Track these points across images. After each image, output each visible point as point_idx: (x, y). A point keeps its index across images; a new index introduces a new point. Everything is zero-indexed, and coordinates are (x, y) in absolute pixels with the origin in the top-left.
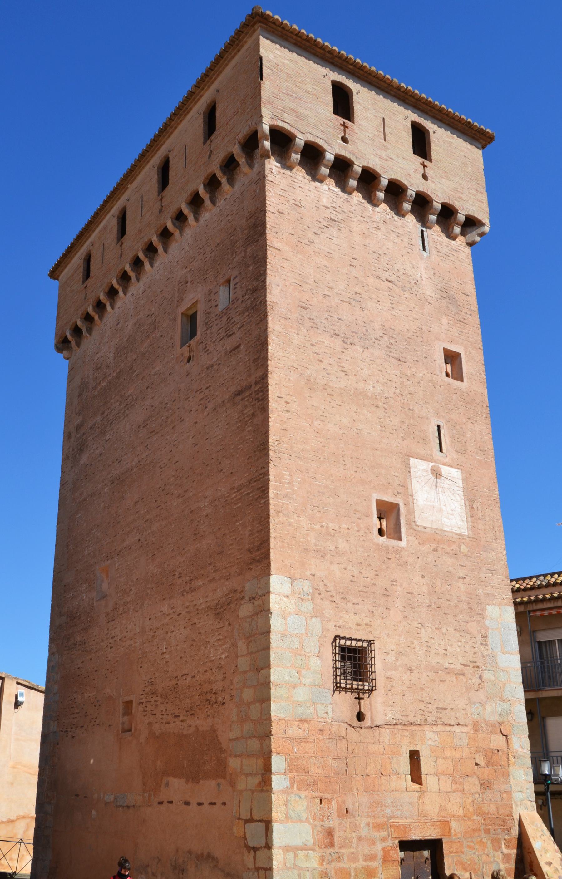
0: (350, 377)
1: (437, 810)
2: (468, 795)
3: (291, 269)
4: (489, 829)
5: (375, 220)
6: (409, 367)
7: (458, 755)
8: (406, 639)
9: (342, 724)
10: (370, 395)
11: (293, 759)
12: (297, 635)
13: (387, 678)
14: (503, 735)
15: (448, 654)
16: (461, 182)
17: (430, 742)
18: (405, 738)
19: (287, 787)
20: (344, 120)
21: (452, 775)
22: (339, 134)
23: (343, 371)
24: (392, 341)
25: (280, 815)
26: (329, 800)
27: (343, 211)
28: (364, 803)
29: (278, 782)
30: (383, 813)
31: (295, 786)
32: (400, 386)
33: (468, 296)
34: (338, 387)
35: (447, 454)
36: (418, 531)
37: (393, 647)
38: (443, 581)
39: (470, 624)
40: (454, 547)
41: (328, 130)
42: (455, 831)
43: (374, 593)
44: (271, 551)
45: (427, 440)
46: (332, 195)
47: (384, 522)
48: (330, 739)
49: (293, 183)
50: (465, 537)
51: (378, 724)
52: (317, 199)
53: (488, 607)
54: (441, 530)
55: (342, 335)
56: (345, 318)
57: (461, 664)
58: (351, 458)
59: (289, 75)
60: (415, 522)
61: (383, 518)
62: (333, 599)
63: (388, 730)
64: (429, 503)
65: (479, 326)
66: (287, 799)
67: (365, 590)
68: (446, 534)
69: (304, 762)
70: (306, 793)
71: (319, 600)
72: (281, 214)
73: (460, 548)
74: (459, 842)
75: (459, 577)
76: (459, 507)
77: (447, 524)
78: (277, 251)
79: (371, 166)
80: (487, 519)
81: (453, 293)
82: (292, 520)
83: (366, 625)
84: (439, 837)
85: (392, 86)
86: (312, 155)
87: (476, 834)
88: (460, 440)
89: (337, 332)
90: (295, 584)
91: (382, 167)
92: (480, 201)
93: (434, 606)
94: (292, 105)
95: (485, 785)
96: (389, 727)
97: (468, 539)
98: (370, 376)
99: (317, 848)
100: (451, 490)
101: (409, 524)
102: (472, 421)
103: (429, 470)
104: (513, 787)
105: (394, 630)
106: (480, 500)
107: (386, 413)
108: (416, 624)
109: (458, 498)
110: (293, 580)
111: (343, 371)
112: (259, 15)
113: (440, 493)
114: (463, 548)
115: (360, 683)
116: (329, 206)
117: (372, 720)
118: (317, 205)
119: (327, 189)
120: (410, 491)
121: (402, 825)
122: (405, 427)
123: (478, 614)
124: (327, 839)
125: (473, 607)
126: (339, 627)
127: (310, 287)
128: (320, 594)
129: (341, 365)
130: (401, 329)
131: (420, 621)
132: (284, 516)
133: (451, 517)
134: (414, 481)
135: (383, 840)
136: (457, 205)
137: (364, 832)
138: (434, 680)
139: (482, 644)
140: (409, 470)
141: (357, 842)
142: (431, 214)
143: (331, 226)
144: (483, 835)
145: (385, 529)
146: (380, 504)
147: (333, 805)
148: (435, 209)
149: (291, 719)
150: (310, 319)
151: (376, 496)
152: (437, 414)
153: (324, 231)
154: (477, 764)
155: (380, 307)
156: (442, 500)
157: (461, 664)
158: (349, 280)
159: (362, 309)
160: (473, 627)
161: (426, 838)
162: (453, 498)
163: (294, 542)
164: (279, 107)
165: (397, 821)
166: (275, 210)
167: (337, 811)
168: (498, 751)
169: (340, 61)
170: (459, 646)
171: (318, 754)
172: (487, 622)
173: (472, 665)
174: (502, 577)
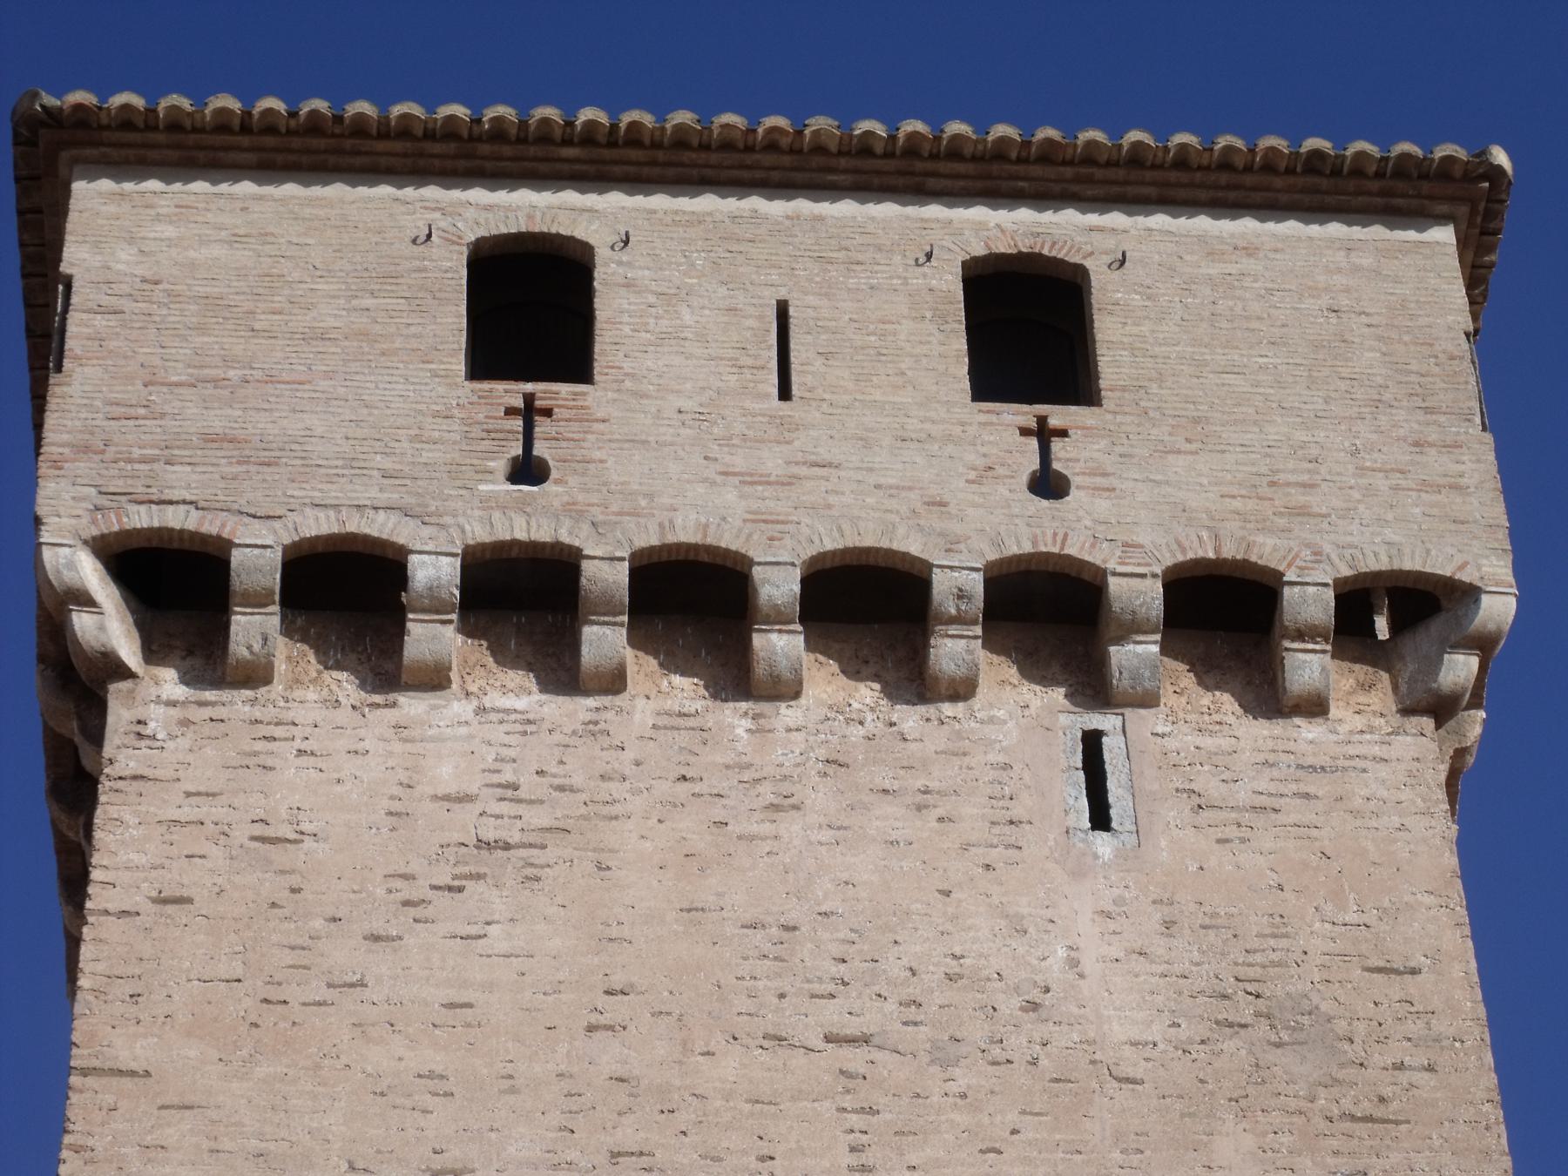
5: (769, 770)
16: (1300, 436)
20: (529, 387)
27: (561, 788)
33: (1414, 972)
41: (426, 456)
46: (498, 733)
49: (260, 746)
52: (403, 776)
65: (1494, 1113)
72: (170, 909)
86: (348, 595)
91: (758, 519)
92: (1439, 489)
94: (217, 422)
112: (43, 124)
118: (396, 806)
119: (470, 715)
136: (1266, 550)
142: (1120, 640)
143: (479, 877)
153: (429, 912)
158: (574, 1104)
164: (137, 452)
166: (138, 901)
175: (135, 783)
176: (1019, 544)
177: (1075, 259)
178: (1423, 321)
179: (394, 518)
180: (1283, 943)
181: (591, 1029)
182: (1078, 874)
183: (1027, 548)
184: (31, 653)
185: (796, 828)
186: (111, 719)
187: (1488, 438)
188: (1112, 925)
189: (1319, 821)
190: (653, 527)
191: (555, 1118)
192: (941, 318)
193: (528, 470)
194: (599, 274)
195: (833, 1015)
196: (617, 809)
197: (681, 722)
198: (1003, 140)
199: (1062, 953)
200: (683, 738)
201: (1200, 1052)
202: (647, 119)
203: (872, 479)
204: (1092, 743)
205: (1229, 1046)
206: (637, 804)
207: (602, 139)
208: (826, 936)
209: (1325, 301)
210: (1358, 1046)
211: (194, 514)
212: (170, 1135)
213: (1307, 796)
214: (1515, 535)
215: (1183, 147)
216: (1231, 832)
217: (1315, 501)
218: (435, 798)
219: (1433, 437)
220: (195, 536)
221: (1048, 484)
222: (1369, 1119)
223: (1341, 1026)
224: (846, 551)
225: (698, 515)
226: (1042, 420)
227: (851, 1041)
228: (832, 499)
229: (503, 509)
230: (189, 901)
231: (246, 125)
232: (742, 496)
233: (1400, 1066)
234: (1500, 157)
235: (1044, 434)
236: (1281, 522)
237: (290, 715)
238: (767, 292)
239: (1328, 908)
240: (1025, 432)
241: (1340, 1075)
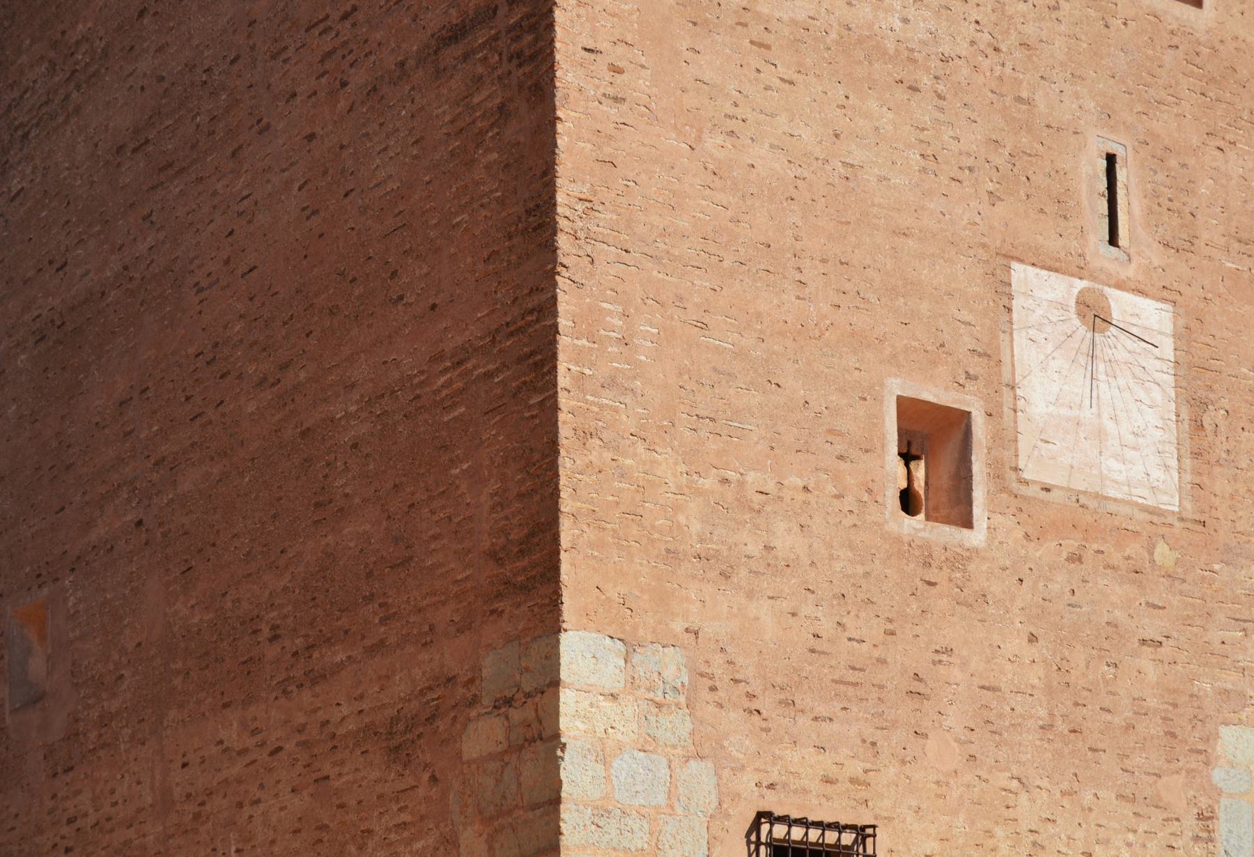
8: (973, 823)
35: (1132, 251)
36: (1025, 498)
39: (1164, 779)
40: (1134, 548)
43: (881, 687)
44: (563, 555)
45: (1072, 203)
47: (919, 470)
50: (1170, 520)
53: (1223, 730)
54: (1097, 496)
58: (824, 261)
60: (1016, 469)
61: (918, 458)
62: (754, 706)
64: (1064, 411)
68: (1112, 507)
71: (711, 708)
73: (1151, 553)
77: (1115, 476)
80: (1243, 465)
82: (629, 462)
90: (636, 659)
93: (1061, 727)
97: (1177, 524)
100: (1138, 371)
105: (938, 796)
106: (1225, 403)
109: (1157, 395)
110: (630, 646)
113: (1102, 377)
114: (1161, 550)
120: (1006, 370)
123: (1191, 751)
125: (1178, 731)
126: (771, 786)
128: (713, 689)
131: (1015, 770)
132: (606, 446)
133: (1130, 454)
134: (1019, 339)
139: (1197, 838)
140: (1005, 301)
145: (922, 492)
146: (909, 409)
151: (897, 386)
160: (1174, 789)
162: (1141, 395)
163: (635, 531)
170: (1129, 845)
172: (1217, 775)
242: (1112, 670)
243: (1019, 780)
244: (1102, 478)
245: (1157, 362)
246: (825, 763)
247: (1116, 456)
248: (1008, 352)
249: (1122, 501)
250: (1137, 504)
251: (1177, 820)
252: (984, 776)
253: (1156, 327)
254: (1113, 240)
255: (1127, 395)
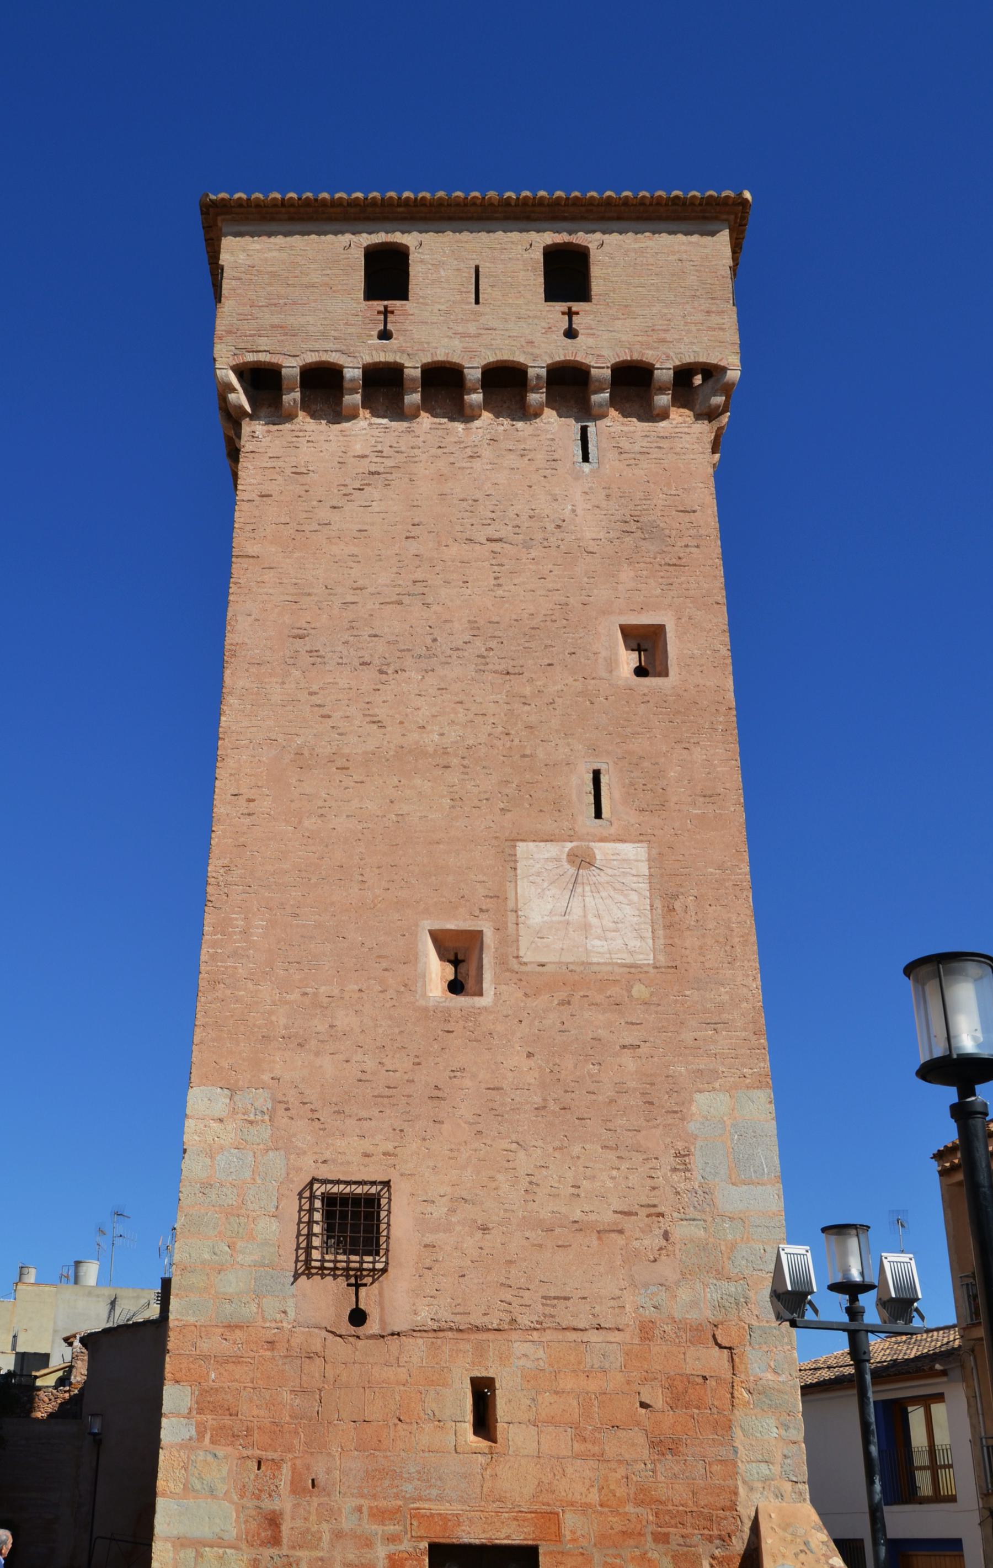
0: (389, 729)
1: (529, 1490)
2: (613, 1465)
3: (278, 581)
4: (667, 1535)
6: (531, 680)
7: (593, 1386)
9: (316, 1330)
10: (431, 750)
11: (207, 1391)
12: (234, 1182)
13: (426, 1246)
14: (721, 1347)
15: (583, 1195)
17: (522, 1362)
18: (461, 1355)
19: (191, 1439)
20: (386, 303)
21: (576, 1426)
22: (371, 329)
23: (374, 722)
24: (493, 644)
25: (171, 1485)
26: (277, 1464)
27: (398, 452)
28: (354, 1472)
29: (173, 1431)
30: (395, 1490)
31: (208, 1437)
32: (505, 719)
33: (694, 511)
34: (360, 752)
36: (523, 973)
37: (446, 1189)
38: (581, 1058)
39: (643, 1133)
41: (349, 331)
42: (573, 1532)
46: (376, 432)
48: (286, 1357)
49: (294, 439)
50: (646, 969)
51: (396, 1329)
53: (697, 1096)
54: (583, 963)
55: (377, 662)
56: (386, 630)
57: (615, 1212)
59: (273, 275)
60: (518, 957)
62: (316, 1115)
63: (420, 1341)
64: (555, 919)
66: (188, 1458)
67: (387, 1094)
69: (229, 1397)
70: (230, 1449)
71: (286, 1120)
72: (265, 499)
73: (629, 991)
74: (582, 1554)
75: (624, 1047)
76: (637, 913)
77: (600, 950)
78: (251, 560)
79: (441, 357)
81: (652, 518)
82: (242, 993)
83: (384, 1154)
84: (530, 1543)
85: (492, 205)
86: (323, 385)
87: (632, 1542)
88: (649, 786)
89: (367, 659)
90: (236, 1098)
92: (714, 329)
93: (552, 1106)
94: (276, 320)
95: (665, 1446)
96: (424, 1334)
97: (652, 971)
98: (433, 716)
99: (244, 1545)
101: (502, 962)
102: (687, 745)
103: (564, 856)
104: (742, 1451)
106: (695, 892)
107: (467, 774)
108: (505, 1144)
109: (634, 897)
110: (233, 1091)
111: (374, 722)
114: (639, 990)
115: (353, 1258)
116: (367, 453)
117: (383, 1322)
118: (341, 460)
120: (511, 904)
121: (440, 1514)
122: (511, 790)
123: (667, 1112)
124: (265, 1530)
125: (655, 1101)
126: (325, 1162)
127: (316, 599)
129: (371, 712)
130: (514, 617)
131: (514, 1137)
132: (228, 987)
133: (610, 935)
135: (391, 1539)
136: (649, 356)
137: (348, 1523)
138: (541, 1246)
139: (675, 1170)
140: (512, 865)
141: (331, 1540)
142: (596, 393)
143: (369, 485)
144: (649, 1542)
147: (284, 1471)
148: (599, 381)
149: (209, 1323)
150: (311, 651)
152: (594, 749)
154: (643, 1405)
155: (469, 592)
156: (589, 907)
157: (615, 1212)
159: (428, 605)
161: (497, 1542)
162: (621, 899)
163: (242, 1029)
165: (427, 1506)
166: (254, 496)
167: (292, 1483)
168: (705, 1378)
169: (378, 210)
171: (259, 1382)
172: (692, 1127)
173: (643, 1212)
174: (744, 1034)
175: (253, 455)
176: (560, 357)
177: (585, 244)
178: (714, 263)
179: (338, 354)
180: (649, 502)
181: (407, 538)
182: (577, 478)
183: (562, 358)
184: (217, 406)
185: (479, 464)
186: (243, 431)
187: (735, 308)
188: (588, 497)
189: (664, 457)
190: (429, 355)
191: (395, 569)
192: (534, 270)
193: (385, 335)
194: (411, 258)
195: (490, 531)
196: (417, 459)
197: (440, 426)
198: (559, 198)
199: (570, 507)
200: (440, 433)
201: (616, 542)
202: (428, 195)
203: (507, 334)
204: (584, 431)
205: (627, 539)
206: (423, 457)
207: (412, 204)
208: (487, 503)
209: (676, 257)
210: (672, 539)
211: (269, 355)
212: (266, 578)
213: (660, 447)
214: (742, 346)
215: (627, 197)
216: (632, 462)
217: (668, 337)
218: (354, 457)
219: (714, 309)
220: (269, 363)
221: (571, 333)
222: (675, 565)
223: (667, 532)
224: (497, 361)
225: (445, 349)
226: (570, 309)
227: (495, 540)
228: (493, 342)
229: (376, 350)
230: (271, 496)
231: (283, 203)
232: (461, 342)
233: (687, 546)
234: (747, 195)
235: (570, 314)
236: (655, 345)
237: (304, 428)
238: (471, 262)
239: (665, 489)
240: (563, 313)
241: (665, 550)
242: (597, 1067)
243: (518, 1143)
244: (587, 952)
245: (635, 879)
246: (366, 1145)
247: (599, 938)
248: (513, 892)
249: (605, 964)
250: (617, 964)
251: (657, 1158)
252: (489, 1142)
253: (633, 858)
254: (598, 814)
255: (608, 901)
